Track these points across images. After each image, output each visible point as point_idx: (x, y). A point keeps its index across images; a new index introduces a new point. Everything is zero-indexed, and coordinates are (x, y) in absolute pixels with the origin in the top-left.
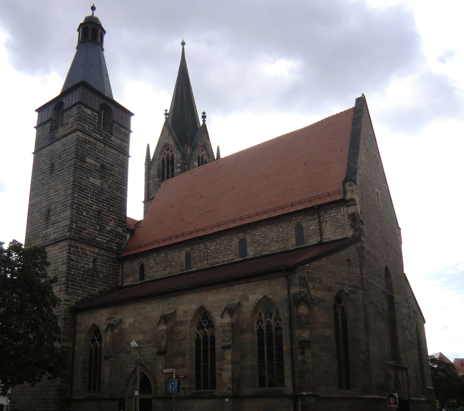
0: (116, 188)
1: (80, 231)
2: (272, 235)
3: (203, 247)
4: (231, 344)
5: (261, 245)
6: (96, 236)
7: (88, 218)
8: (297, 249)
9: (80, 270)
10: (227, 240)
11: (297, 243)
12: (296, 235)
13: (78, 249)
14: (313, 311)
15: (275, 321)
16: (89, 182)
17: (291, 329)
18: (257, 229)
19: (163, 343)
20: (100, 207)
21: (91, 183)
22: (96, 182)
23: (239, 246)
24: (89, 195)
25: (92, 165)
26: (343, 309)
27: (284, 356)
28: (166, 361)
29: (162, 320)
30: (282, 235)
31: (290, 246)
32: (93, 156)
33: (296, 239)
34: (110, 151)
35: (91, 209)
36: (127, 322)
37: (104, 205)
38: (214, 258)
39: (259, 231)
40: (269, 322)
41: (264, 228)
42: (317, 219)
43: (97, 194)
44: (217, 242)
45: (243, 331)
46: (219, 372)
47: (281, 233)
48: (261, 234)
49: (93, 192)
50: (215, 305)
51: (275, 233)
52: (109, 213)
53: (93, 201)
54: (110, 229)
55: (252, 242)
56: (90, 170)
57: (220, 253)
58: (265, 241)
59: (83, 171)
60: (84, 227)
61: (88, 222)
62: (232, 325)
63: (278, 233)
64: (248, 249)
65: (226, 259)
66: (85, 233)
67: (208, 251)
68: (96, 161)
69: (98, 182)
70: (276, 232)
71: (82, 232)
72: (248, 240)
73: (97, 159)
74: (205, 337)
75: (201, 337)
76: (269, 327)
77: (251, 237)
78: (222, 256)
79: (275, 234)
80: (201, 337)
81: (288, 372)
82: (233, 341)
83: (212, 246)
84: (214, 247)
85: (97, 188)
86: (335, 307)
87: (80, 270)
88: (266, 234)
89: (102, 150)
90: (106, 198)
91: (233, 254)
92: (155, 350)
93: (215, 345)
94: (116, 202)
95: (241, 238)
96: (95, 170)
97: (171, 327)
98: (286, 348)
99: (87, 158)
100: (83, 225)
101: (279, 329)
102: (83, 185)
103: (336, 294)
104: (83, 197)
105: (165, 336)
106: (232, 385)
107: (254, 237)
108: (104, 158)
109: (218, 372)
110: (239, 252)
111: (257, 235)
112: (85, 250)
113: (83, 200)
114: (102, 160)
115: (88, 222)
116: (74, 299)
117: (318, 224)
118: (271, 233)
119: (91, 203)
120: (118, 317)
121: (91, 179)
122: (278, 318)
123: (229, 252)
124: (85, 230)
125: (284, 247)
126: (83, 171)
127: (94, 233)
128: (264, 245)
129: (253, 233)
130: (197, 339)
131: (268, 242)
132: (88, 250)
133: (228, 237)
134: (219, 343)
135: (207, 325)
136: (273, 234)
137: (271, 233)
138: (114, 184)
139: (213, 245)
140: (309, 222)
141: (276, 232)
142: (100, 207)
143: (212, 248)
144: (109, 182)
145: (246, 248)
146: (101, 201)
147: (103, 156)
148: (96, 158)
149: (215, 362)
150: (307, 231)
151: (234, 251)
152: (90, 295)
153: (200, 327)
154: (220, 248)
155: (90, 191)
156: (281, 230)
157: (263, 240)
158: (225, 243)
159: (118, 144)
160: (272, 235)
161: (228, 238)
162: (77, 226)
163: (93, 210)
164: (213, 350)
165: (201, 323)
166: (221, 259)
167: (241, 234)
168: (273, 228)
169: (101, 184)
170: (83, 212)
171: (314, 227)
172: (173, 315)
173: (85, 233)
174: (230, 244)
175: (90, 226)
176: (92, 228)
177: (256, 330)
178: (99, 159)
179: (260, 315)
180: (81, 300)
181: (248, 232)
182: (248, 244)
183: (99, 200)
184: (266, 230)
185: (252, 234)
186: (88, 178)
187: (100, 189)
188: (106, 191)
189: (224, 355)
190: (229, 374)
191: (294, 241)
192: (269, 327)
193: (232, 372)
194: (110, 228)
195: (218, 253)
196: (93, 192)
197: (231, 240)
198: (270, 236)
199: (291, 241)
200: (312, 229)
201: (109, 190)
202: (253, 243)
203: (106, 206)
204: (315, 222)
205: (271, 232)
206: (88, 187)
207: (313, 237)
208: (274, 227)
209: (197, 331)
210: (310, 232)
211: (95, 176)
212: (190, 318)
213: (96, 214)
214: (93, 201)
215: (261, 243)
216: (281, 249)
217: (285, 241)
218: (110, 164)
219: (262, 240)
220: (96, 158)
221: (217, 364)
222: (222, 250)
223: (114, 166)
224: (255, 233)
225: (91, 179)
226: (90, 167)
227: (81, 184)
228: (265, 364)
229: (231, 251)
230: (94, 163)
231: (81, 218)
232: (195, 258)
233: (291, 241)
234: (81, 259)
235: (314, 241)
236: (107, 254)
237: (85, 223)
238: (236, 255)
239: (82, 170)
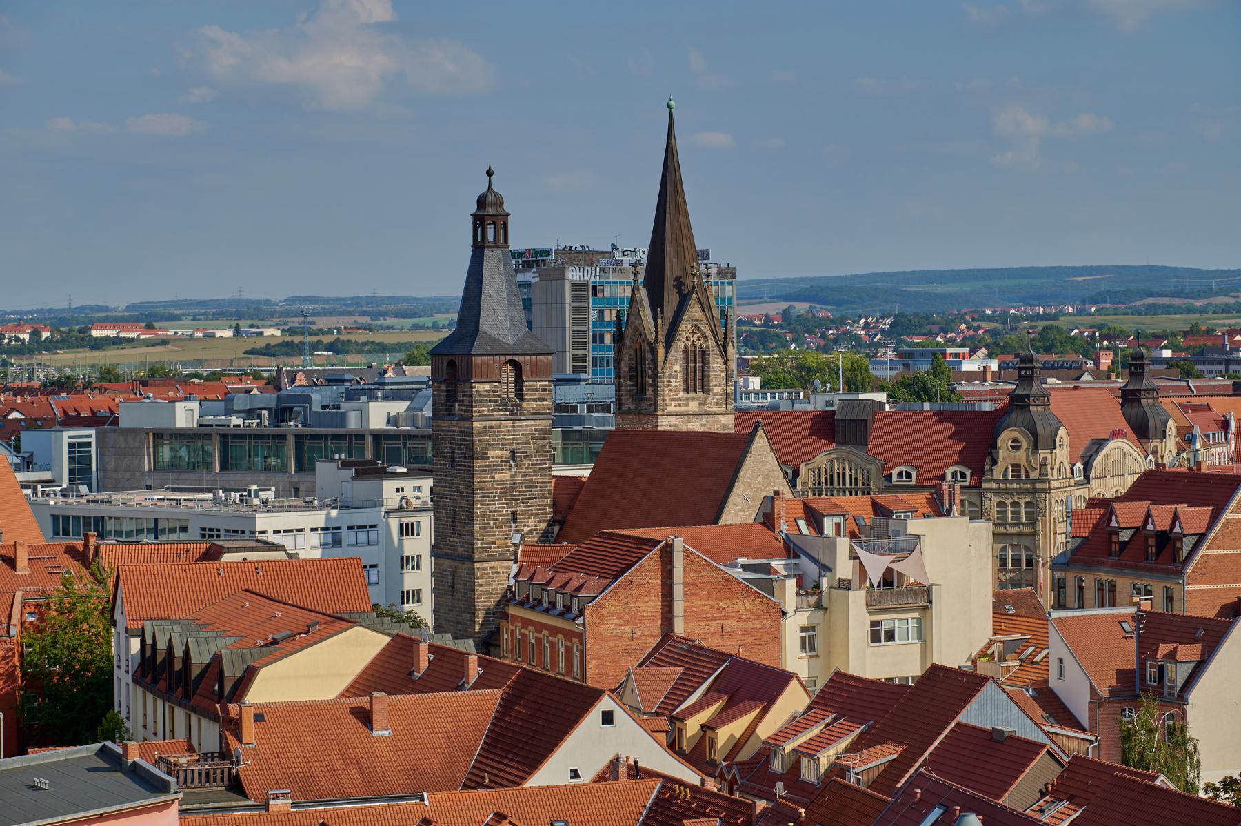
22: (505, 477)
25: (498, 457)
35: (499, 516)
43: (507, 492)
49: (501, 492)
53: (502, 504)
68: (502, 450)
85: (507, 484)
87: (492, 594)
90: (520, 491)
96: (502, 461)
102: (488, 489)
104: (488, 505)
112: (497, 568)
113: (489, 508)
121: (497, 477)
124: (494, 543)
146: (513, 499)
148: (502, 444)
159: (533, 409)
169: (512, 476)
178: (505, 444)
183: (510, 499)
186: (493, 477)
206: (494, 489)
211: (502, 470)
214: (502, 504)
218: (522, 444)
220: (502, 444)
225: (497, 477)
231: (487, 532)
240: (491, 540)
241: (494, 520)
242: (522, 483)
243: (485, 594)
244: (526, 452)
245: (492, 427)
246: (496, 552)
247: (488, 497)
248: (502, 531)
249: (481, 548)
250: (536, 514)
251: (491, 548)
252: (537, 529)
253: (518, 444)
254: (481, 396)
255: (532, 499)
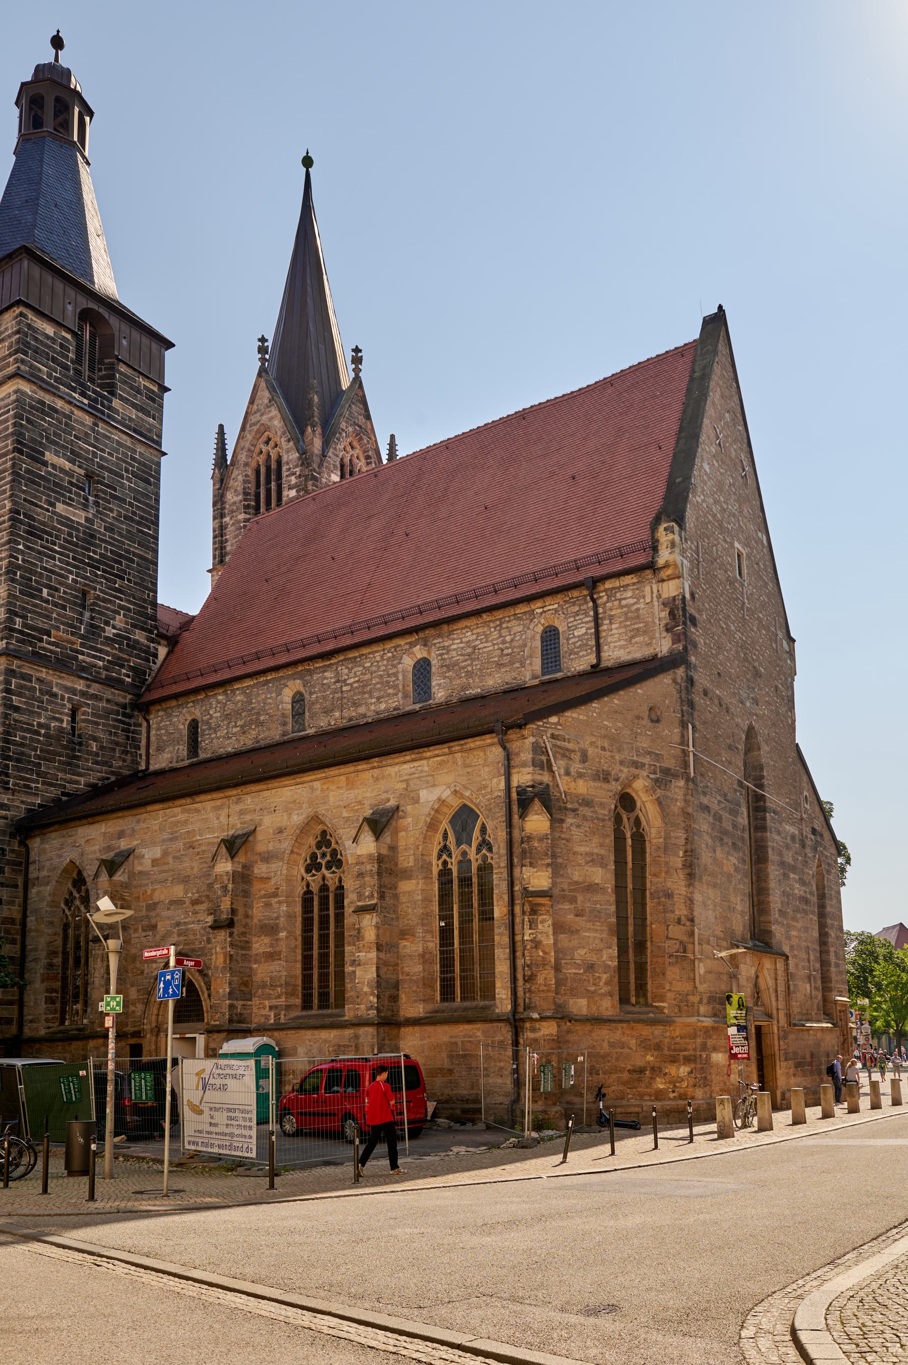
0: (128, 531)
1: (34, 637)
2: (488, 649)
3: (331, 678)
4: (376, 905)
5: (463, 675)
6: (77, 652)
7: (56, 605)
8: (543, 683)
9: (39, 734)
10: (385, 662)
11: (545, 669)
12: (542, 651)
13: (31, 681)
14: (564, 825)
15: (479, 850)
16: (54, 513)
17: (511, 866)
18: (455, 636)
19: (226, 904)
20: (86, 578)
21: (60, 515)
22: (74, 514)
23: (414, 675)
24: (56, 548)
25: (62, 470)
26: (637, 822)
27: (496, 931)
28: (231, 945)
29: (223, 850)
30: (510, 651)
31: (528, 676)
32: (63, 447)
33: (543, 660)
34: (109, 438)
35: (61, 584)
36: (146, 856)
37: (97, 575)
38: (356, 705)
39: (459, 641)
40: (464, 854)
41: (469, 634)
42: (592, 613)
43: (76, 545)
44: (364, 668)
45: (406, 874)
46: (351, 969)
47: (508, 645)
48: (462, 648)
49: (66, 540)
50: (345, 814)
51: (494, 645)
52: (111, 595)
53: (68, 564)
54: (114, 635)
55: (442, 666)
56: (56, 484)
57: (370, 693)
58: (471, 665)
59: (39, 485)
60: (46, 627)
61: (54, 615)
62: (380, 859)
63: (501, 646)
64: (433, 684)
65: (383, 706)
66: (49, 643)
67: (344, 689)
68: (72, 462)
69: (79, 516)
70: (497, 644)
71: (41, 640)
72: (434, 662)
73: (74, 456)
74: (324, 888)
75: (315, 888)
76: (465, 862)
77: (441, 655)
78: (374, 700)
79: (496, 647)
80: (315, 888)
81: (502, 967)
82: (382, 896)
83: (352, 675)
84: (357, 679)
85: (78, 530)
86: (618, 820)
88: (474, 648)
89: (86, 433)
90: (101, 555)
91: (400, 695)
92: (210, 919)
93: (343, 907)
94: (128, 567)
95: (419, 656)
96: (71, 483)
97: (244, 867)
98: (499, 911)
99: (47, 453)
100: (41, 623)
101: (485, 869)
103: (619, 788)
104: (39, 552)
105: (230, 886)
106: (378, 997)
107: (447, 653)
108: (94, 454)
109: (348, 969)
110: (414, 690)
111: (454, 650)
112: (50, 684)
113: (41, 561)
114: (86, 459)
115: (54, 615)
116: (22, 802)
117: (592, 624)
118: (485, 645)
119: (61, 568)
120: (124, 844)
122: (485, 844)
123: (391, 691)
125: (515, 679)
126: (39, 485)
127: (74, 643)
128: (469, 674)
129: (446, 644)
130: (305, 893)
131: (478, 667)
132: (57, 684)
133: (390, 655)
134: (351, 900)
135: (328, 862)
136: (491, 648)
137: (485, 645)
138: (122, 523)
139: (355, 673)
140: (572, 619)
141: (497, 644)
142: (86, 578)
143: (352, 680)
144: (107, 515)
145: (429, 680)
147: (91, 449)
148: (72, 452)
149: (343, 946)
150: (568, 639)
151: (401, 687)
152: (63, 794)
153: (313, 866)
154: (371, 680)
155: (57, 537)
156: (508, 638)
157: (469, 662)
158: (383, 668)
159: (130, 419)
160: (488, 649)
161: (389, 658)
162: (25, 625)
163: (67, 586)
164: (340, 917)
165: (314, 856)
166: (373, 708)
167: (418, 647)
168: (491, 632)
169: (87, 519)
170: (41, 591)
171: (583, 631)
172: (251, 838)
173: (49, 643)
174: (394, 670)
175: (62, 627)
176: (65, 631)
177: (435, 871)
178: (79, 455)
179: (445, 836)
180: (40, 806)
181: (436, 641)
182: (434, 669)
183: (83, 562)
184: (474, 637)
185: (444, 648)
186: (53, 505)
187: (84, 533)
188: (100, 540)
189: (359, 930)
190: (372, 974)
191: (537, 664)
192: (465, 862)
193: (378, 968)
194: (115, 631)
195: (365, 693)
196: (66, 540)
197: (396, 662)
198: (484, 653)
199: (531, 664)
200: (579, 636)
201: (110, 537)
202: (445, 669)
203: (102, 577)
204: (588, 619)
205: (487, 642)
206: (54, 528)
207: (581, 654)
208: (492, 630)
209: (305, 875)
210: (574, 643)
211: (71, 499)
212: (286, 845)
213: (76, 597)
214: (68, 564)
215: (464, 668)
216: (507, 683)
217: (518, 665)
218: (110, 471)
219: (466, 661)
220: (72, 452)
221: (348, 949)
222: (375, 684)
223: (122, 477)
224: (450, 645)
225: (60, 508)
226: (55, 475)
227: (34, 519)
228: (453, 950)
229: (395, 687)
230: (67, 465)
231: (36, 605)
232: (313, 703)
233: (531, 664)
234: (38, 707)
235: (581, 662)
236: (108, 693)
237: (49, 618)
238: (405, 696)
239: (34, 482)
240: (40, 625)
241: (49, 587)
242: (105, 542)
243: (25, 730)
244: (115, 490)
245: (56, 410)
246: (51, 651)
247: (42, 539)
248: (65, 616)
249: (21, 632)
250: (129, 610)
251: (41, 640)
252: (129, 639)
253: (101, 467)
254: (36, 339)
255: (123, 578)
